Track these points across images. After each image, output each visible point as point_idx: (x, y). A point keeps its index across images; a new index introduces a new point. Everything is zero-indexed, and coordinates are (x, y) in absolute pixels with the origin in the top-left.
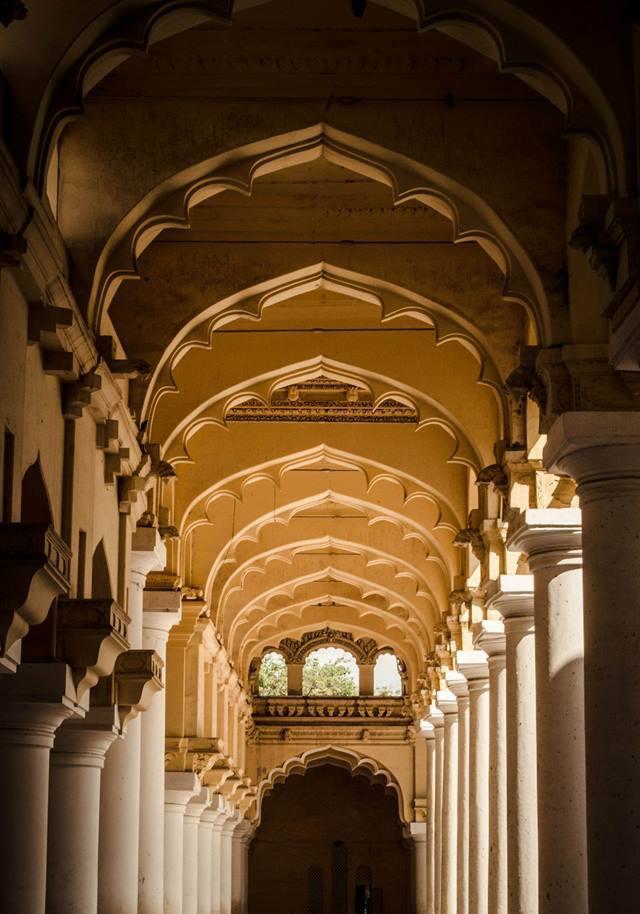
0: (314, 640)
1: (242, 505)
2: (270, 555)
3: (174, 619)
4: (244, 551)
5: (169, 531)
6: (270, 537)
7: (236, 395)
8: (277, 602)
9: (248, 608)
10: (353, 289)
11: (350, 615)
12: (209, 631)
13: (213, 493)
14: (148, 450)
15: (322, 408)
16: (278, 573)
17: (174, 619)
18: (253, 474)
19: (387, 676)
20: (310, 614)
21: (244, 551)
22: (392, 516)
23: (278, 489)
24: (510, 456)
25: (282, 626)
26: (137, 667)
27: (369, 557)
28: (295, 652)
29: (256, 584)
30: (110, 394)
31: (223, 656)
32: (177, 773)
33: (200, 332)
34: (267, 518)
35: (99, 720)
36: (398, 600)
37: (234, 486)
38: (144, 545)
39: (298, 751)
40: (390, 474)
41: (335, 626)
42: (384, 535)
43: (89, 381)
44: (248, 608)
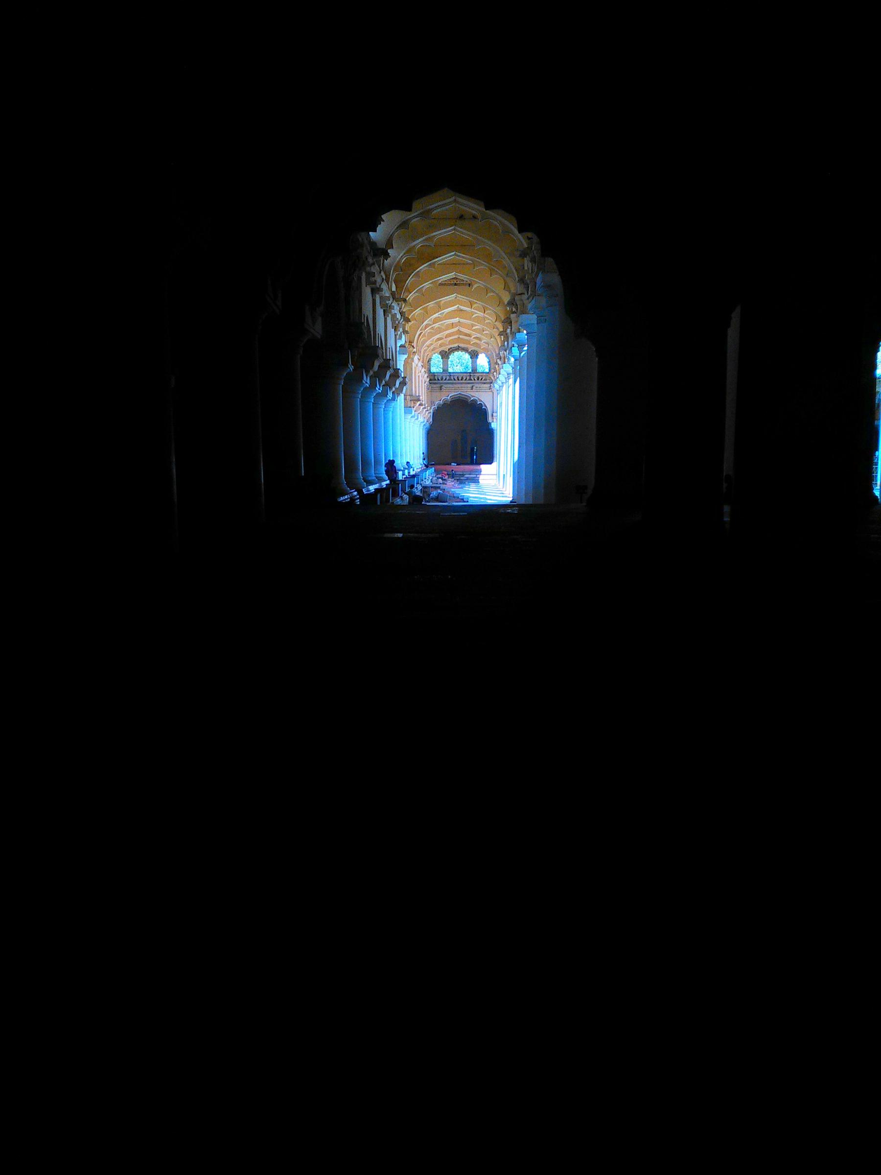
0: (452, 350)
1: (427, 313)
2: (436, 325)
3: (406, 356)
4: (426, 327)
5: (405, 332)
6: (436, 321)
7: (427, 285)
8: (439, 339)
9: (428, 343)
10: (465, 258)
11: (468, 342)
12: (416, 358)
13: (418, 311)
14: (402, 314)
15: (455, 284)
16: (439, 330)
17: (406, 356)
18: (431, 304)
19: (483, 362)
20: (450, 342)
21: (426, 327)
22: (481, 314)
23: (439, 308)
24: (513, 316)
25: (441, 346)
26: (403, 383)
27: (473, 326)
28: (445, 355)
29: (431, 335)
30: (396, 310)
31: (420, 364)
32: (408, 409)
33: (417, 275)
34: (436, 315)
35: (394, 399)
36: (485, 339)
37: (425, 309)
38: (400, 338)
39: (447, 394)
40: (478, 304)
41: (462, 345)
42: (478, 320)
43: (391, 307)
44: (428, 343)
